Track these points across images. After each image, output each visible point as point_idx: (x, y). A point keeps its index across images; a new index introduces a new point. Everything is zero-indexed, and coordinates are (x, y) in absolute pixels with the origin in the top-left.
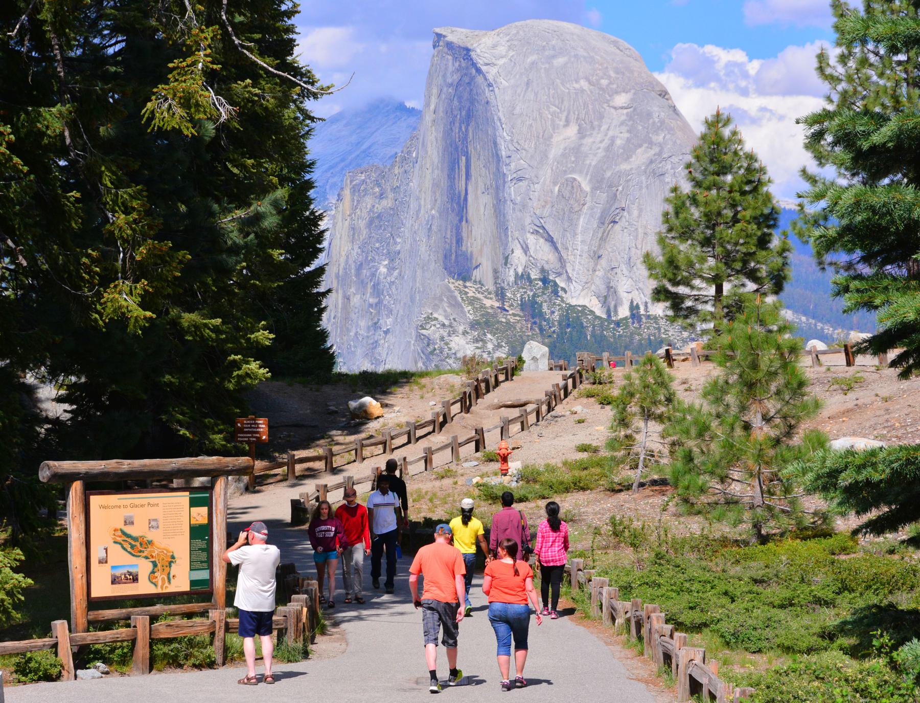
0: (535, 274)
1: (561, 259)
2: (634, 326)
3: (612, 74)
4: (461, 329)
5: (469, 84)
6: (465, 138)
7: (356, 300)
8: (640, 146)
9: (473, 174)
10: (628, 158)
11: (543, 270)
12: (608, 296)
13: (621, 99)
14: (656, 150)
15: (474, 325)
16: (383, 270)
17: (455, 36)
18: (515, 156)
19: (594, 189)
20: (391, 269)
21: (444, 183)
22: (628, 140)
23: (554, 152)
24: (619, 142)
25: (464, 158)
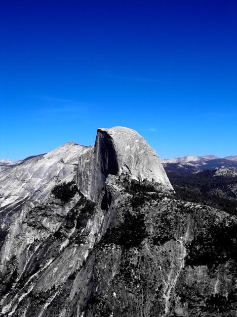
0: (125, 173)
7: (83, 179)
12: (139, 177)
13: (137, 141)
15: (117, 183)
16: (88, 173)
17: (103, 129)
20: (90, 173)
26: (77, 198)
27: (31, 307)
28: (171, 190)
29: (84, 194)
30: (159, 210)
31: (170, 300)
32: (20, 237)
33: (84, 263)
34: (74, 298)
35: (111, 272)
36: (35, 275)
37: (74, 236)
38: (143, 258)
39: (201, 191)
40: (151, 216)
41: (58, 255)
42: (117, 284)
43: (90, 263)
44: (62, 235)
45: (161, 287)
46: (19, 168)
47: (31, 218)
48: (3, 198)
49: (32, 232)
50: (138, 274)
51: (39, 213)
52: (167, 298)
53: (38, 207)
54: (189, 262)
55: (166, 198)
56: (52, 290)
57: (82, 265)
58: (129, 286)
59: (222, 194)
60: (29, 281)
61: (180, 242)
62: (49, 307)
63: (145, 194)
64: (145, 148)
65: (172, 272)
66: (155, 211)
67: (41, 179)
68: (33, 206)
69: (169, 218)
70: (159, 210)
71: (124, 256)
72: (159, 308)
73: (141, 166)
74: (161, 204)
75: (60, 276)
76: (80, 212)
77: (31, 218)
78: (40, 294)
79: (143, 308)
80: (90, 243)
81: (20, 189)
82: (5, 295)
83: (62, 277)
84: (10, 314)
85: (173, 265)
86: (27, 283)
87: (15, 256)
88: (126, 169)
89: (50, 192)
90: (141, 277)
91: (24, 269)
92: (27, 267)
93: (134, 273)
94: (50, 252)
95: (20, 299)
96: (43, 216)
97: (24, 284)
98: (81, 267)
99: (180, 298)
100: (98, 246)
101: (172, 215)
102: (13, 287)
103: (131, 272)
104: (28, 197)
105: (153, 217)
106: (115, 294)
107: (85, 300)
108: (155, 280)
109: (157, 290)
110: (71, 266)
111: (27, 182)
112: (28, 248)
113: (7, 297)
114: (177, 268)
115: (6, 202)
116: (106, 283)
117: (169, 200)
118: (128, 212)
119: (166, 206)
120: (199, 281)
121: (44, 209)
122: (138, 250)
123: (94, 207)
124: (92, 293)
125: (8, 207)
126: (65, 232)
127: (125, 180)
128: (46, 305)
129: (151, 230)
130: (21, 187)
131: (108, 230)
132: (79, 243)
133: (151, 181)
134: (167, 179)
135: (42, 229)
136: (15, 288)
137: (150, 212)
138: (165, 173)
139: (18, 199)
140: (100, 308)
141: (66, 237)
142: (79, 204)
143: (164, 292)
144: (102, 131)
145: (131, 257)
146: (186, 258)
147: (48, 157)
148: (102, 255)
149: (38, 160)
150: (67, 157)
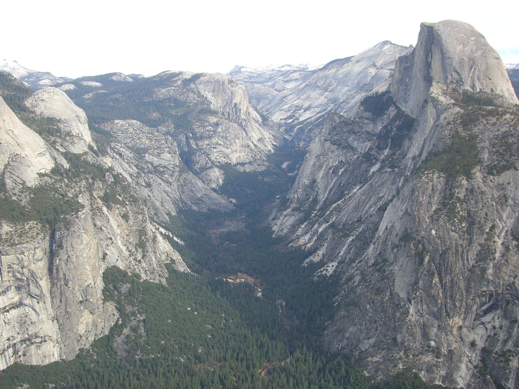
0: (454, 81)
1: (461, 78)
2: (481, 94)
3: (470, 32)
4: (440, 94)
5: (432, 35)
6: (431, 48)
7: (401, 88)
8: (479, 50)
9: (433, 57)
10: (476, 53)
11: (457, 81)
13: (472, 39)
14: (484, 51)
15: (443, 94)
16: (407, 80)
18: (447, 53)
19: (469, 60)
20: (409, 80)
21: (424, 60)
22: (476, 48)
23: (457, 52)
24: (474, 49)
25: (430, 53)
26: (392, 112)
27: (333, 239)
28: (516, 104)
29: (401, 107)
30: (498, 130)
31: (502, 244)
32: (321, 157)
33: (398, 193)
34: (384, 232)
35: (431, 205)
36: (338, 203)
37: (387, 158)
40: (486, 137)
41: (366, 181)
42: (437, 220)
43: (406, 191)
44: (372, 157)
45: (493, 227)
46: (321, 74)
47: (335, 135)
48: (302, 111)
49: (336, 153)
50: (465, 210)
51: (345, 130)
52: (499, 242)
53: (343, 122)
55: (508, 116)
56: (358, 221)
57: (394, 193)
58: (452, 223)
60: (331, 209)
62: (352, 241)
63: (480, 109)
64: (484, 48)
66: (492, 131)
67: (347, 88)
68: (338, 121)
69: (510, 141)
70: (498, 130)
71: (449, 186)
72: (489, 252)
73: (477, 73)
74: (501, 123)
75: (368, 206)
76: (395, 129)
77: (335, 135)
78: (344, 225)
79: (469, 250)
80: (407, 168)
81: (322, 100)
82: (303, 224)
83: (370, 207)
84: (309, 245)
85: (510, 202)
86: (329, 212)
87: (316, 180)
88: (456, 76)
89: (359, 104)
90: (468, 213)
91: (326, 195)
92: (329, 194)
93: (459, 208)
94: (357, 177)
95: (320, 230)
96: (349, 133)
97: (325, 213)
98: (394, 197)
99: (517, 243)
100: (417, 171)
101: (515, 138)
102: (313, 215)
103: (456, 207)
104: (332, 109)
105: (490, 140)
106: (433, 232)
107: (397, 235)
108: (486, 219)
109: (488, 230)
110: (381, 195)
111: (330, 92)
112: (331, 171)
113: (306, 226)
115: (305, 116)
116: (424, 219)
117: (512, 117)
118: (457, 132)
119: (507, 125)
121: (350, 124)
122: (467, 181)
123: (413, 123)
124: (406, 230)
125: (308, 121)
126: (376, 154)
127: (454, 90)
128: (350, 239)
129: (486, 156)
130: (323, 98)
131: (430, 153)
132: (393, 167)
133: (489, 92)
134: (512, 90)
135: (347, 149)
136: (315, 216)
138: (510, 82)
139: (320, 112)
140: (414, 247)
141: (377, 160)
142: (394, 119)
143: (497, 234)
144: (426, 26)
145: (457, 188)
147: (357, 60)
148: (420, 184)
149: (344, 64)
150: (380, 60)
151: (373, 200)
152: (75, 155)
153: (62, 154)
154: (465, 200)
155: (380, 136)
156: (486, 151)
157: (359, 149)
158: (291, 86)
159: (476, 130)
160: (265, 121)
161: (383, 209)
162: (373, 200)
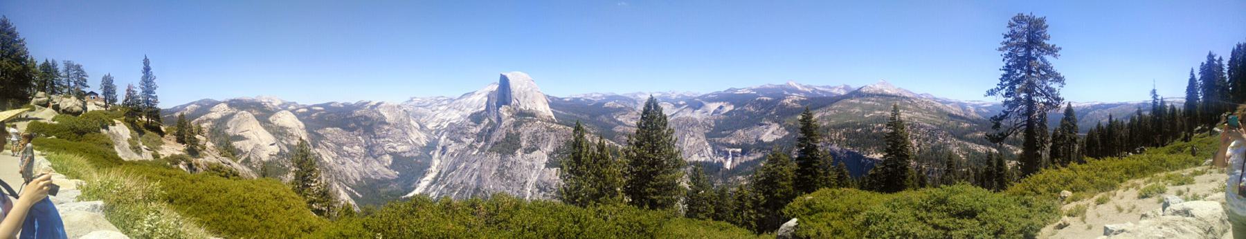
26: (487, 121)
38: (515, 162)
39: (590, 117)
45: (526, 182)
49: (454, 145)
51: (459, 132)
54: (548, 165)
59: (606, 119)
61: (545, 152)
65: (535, 172)
73: (527, 99)
81: (458, 116)
85: (536, 167)
106: (491, 186)
114: (539, 169)
118: (510, 131)
120: (552, 178)
127: (515, 109)
129: (524, 144)
137: (526, 132)
138: (547, 105)
146: (546, 163)
151: (470, 171)
152: (293, 146)
153: (285, 145)
154: (511, 168)
155: (478, 135)
156: (525, 141)
157: (467, 143)
158: (441, 108)
159: (520, 130)
160: (422, 127)
161: (472, 176)
162: (470, 171)
